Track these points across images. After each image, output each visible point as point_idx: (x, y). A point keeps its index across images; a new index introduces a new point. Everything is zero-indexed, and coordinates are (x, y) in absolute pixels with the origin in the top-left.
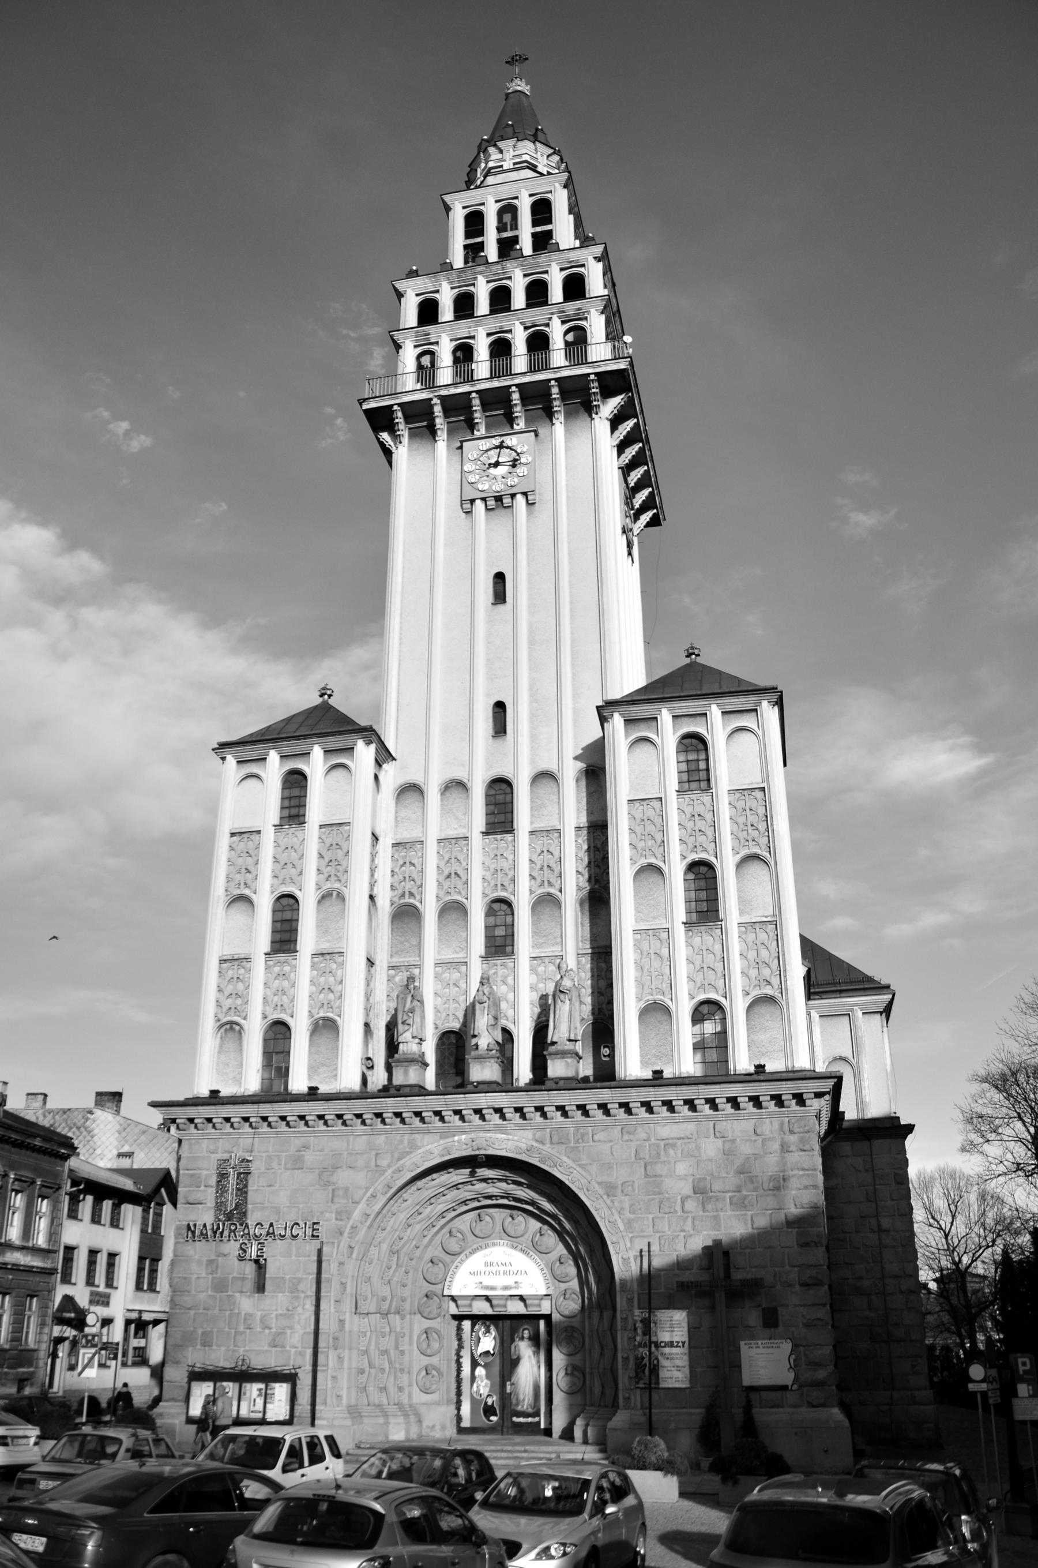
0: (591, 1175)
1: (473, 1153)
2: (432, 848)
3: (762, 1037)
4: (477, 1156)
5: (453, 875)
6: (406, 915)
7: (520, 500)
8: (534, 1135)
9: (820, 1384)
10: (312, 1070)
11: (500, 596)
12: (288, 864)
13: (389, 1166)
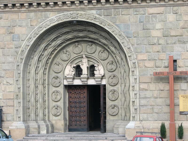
0: (120, 29)
1: (71, 20)
4: (73, 21)
8: (97, 12)
13: (36, 25)
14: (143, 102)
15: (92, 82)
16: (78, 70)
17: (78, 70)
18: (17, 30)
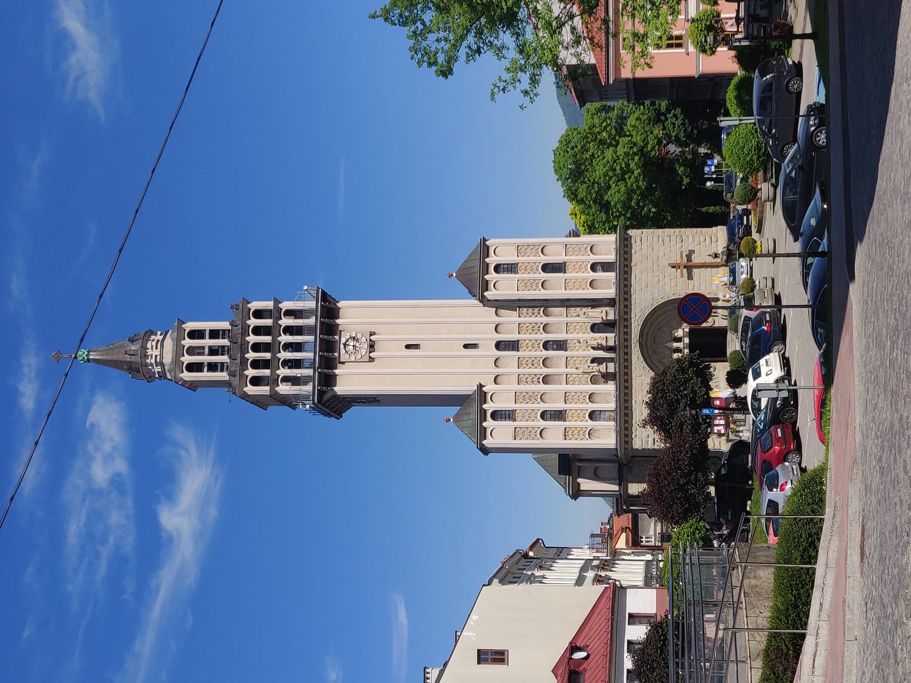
2: (521, 370)
3: (604, 251)
6: (546, 380)
7: (373, 338)
10: (607, 402)
11: (416, 346)
15: (687, 340)
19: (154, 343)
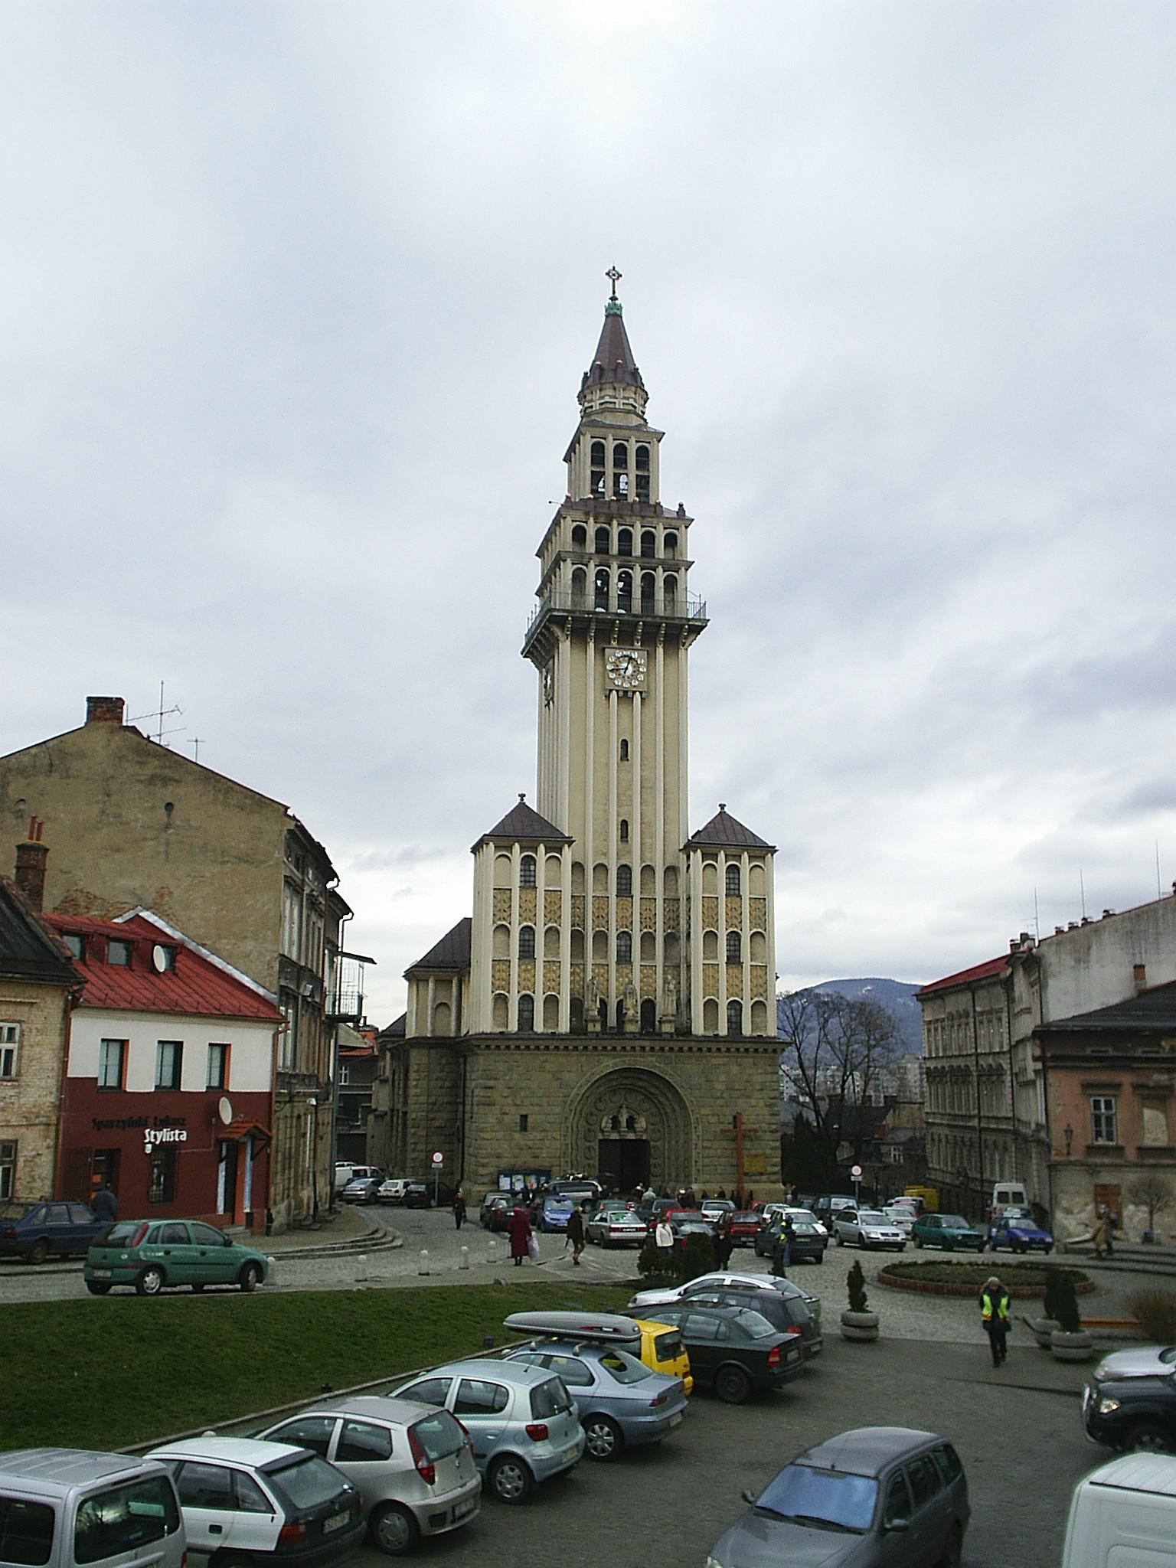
2: (590, 900)
3: (758, 1020)
5: (602, 917)
6: (578, 937)
9: (774, 1173)
11: (624, 756)
12: (528, 912)
14: (707, 1161)
15: (631, 1136)
16: (615, 1122)
17: (615, 1122)
18: (566, 1076)
19: (631, 401)
